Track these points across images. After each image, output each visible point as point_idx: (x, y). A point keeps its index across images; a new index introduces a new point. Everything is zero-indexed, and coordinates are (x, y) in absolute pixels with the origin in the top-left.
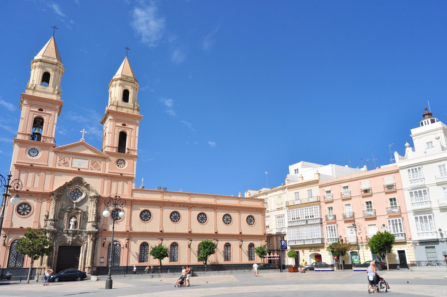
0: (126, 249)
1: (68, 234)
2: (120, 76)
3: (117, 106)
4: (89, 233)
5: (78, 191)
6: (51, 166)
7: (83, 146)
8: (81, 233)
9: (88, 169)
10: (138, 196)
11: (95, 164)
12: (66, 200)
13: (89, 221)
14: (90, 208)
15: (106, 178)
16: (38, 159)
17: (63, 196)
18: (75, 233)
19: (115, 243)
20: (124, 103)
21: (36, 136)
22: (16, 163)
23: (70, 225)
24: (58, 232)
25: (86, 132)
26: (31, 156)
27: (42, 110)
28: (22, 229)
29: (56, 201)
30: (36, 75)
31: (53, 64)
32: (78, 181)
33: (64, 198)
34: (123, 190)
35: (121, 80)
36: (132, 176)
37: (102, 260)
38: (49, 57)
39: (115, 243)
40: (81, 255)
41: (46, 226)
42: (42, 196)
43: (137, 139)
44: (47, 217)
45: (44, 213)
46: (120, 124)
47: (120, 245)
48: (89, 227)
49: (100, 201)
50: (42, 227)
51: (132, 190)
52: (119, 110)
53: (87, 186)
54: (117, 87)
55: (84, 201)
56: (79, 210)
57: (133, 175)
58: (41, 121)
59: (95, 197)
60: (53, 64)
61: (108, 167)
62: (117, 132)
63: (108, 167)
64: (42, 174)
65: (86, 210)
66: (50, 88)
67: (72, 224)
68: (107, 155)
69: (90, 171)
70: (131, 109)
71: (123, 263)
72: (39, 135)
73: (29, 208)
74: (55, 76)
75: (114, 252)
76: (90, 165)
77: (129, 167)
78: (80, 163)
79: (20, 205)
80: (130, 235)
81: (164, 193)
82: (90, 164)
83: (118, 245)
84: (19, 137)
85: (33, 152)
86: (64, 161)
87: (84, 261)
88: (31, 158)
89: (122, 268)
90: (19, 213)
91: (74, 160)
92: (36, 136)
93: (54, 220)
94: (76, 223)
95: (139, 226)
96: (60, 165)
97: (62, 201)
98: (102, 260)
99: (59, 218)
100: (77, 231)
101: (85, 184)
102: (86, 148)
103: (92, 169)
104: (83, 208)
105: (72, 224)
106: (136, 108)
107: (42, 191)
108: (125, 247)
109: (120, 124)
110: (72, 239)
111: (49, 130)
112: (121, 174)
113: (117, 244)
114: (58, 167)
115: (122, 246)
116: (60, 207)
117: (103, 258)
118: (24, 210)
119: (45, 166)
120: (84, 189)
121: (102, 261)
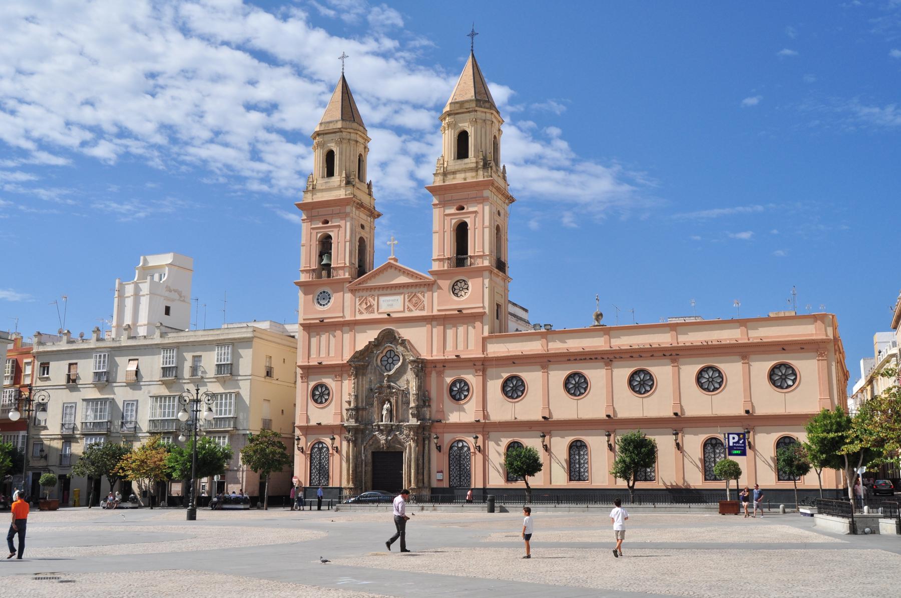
0: (479, 456)
1: (381, 431)
4: (410, 428)
6: (348, 317)
7: (393, 270)
8: (399, 428)
9: (404, 311)
10: (497, 349)
11: (414, 300)
14: (410, 382)
15: (434, 323)
18: (389, 430)
19: (460, 445)
22: (302, 322)
32: (388, 337)
34: (467, 342)
36: (481, 310)
37: (440, 476)
40: (405, 467)
42: (337, 371)
46: (453, 210)
49: (423, 367)
51: (484, 339)
53: (403, 343)
55: (401, 372)
57: (483, 307)
59: (414, 361)
61: (439, 301)
63: (439, 301)
64: (338, 333)
69: (407, 314)
71: (477, 482)
72: (328, 267)
75: (459, 462)
76: (407, 303)
78: (390, 303)
79: (315, 388)
80: (485, 428)
81: (549, 336)
82: (407, 300)
83: (466, 449)
85: (324, 297)
90: (316, 401)
91: (382, 299)
94: (390, 411)
95: (502, 410)
96: (361, 313)
97: (369, 375)
98: (440, 476)
99: (367, 404)
102: (397, 271)
103: (410, 310)
104: (402, 384)
110: (386, 440)
112: (460, 311)
113: (463, 446)
115: (472, 450)
117: (442, 472)
119: (341, 319)
120: (400, 349)
121: (439, 478)
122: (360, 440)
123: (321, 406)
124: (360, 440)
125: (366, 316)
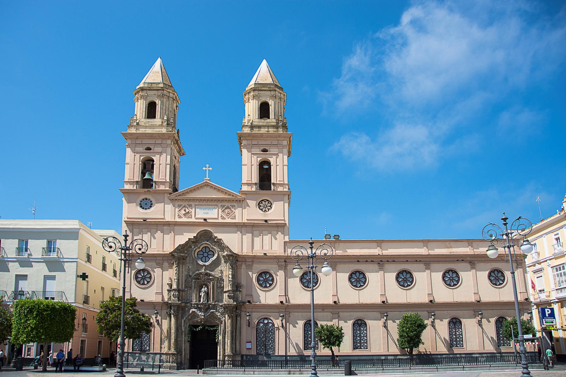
0: (282, 331)
2: (253, 86)
7: (208, 188)
8: (214, 307)
9: (217, 219)
12: (193, 263)
13: (225, 290)
14: (225, 272)
15: (244, 229)
16: (152, 211)
17: (188, 258)
18: (206, 308)
19: (266, 322)
20: (263, 121)
21: (147, 184)
22: (127, 220)
24: (186, 306)
25: (211, 169)
26: (143, 208)
27: (150, 149)
28: (142, 303)
29: (178, 266)
30: (140, 108)
31: (158, 90)
32: (206, 236)
33: (190, 260)
34: (272, 245)
35: (254, 90)
36: (283, 222)
37: (249, 346)
38: (152, 83)
39: (266, 322)
41: (170, 299)
42: (162, 260)
43: (286, 168)
44: (171, 286)
45: (166, 281)
46: (258, 151)
47: (273, 325)
48: (226, 300)
50: (166, 300)
52: (256, 131)
53: (219, 243)
54: (250, 101)
55: (217, 263)
56: (210, 275)
57: (284, 220)
58: (151, 163)
60: (158, 90)
62: (256, 161)
65: (220, 275)
66: (157, 121)
67: (202, 294)
68: (243, 196)
69: (220, 220)
70: (273, 126)
71: (280, 351)
73: (149, 276)
74: (162, 103)
75: (265, 336)
76: (220, 213)
77: (278, 211)
80: (286, 310)
81: (337, 245)
83: (270, 325)
84: (127, 187)
85: (146, 204)
86: (185, 211)
87: (225, 348)
88: (144, 211)
89: (278, 359)
92: (147, 184)
93: (178, 290)
94: (207, 294)
95: (299, 296)
96: (180, 217)
98: (249, 346)
99: (186, 287)
100: (210, 304)
102: (212, 190)
103: (223, 218)
104: (216, 273)
105: (202, 294)
106: (280, 124)
107: (162, 253)
108: (281, 328)
109: (258, 151)
111: (161, 173)
114: (177, 220)
115: (276, 326)
116: (185, 273)
117: (250, 342)
118: (144, 278)
121: (249, 346)
122: (180, 315)
123: (143, 286)
124: (180, 315)
125: (184, 219)
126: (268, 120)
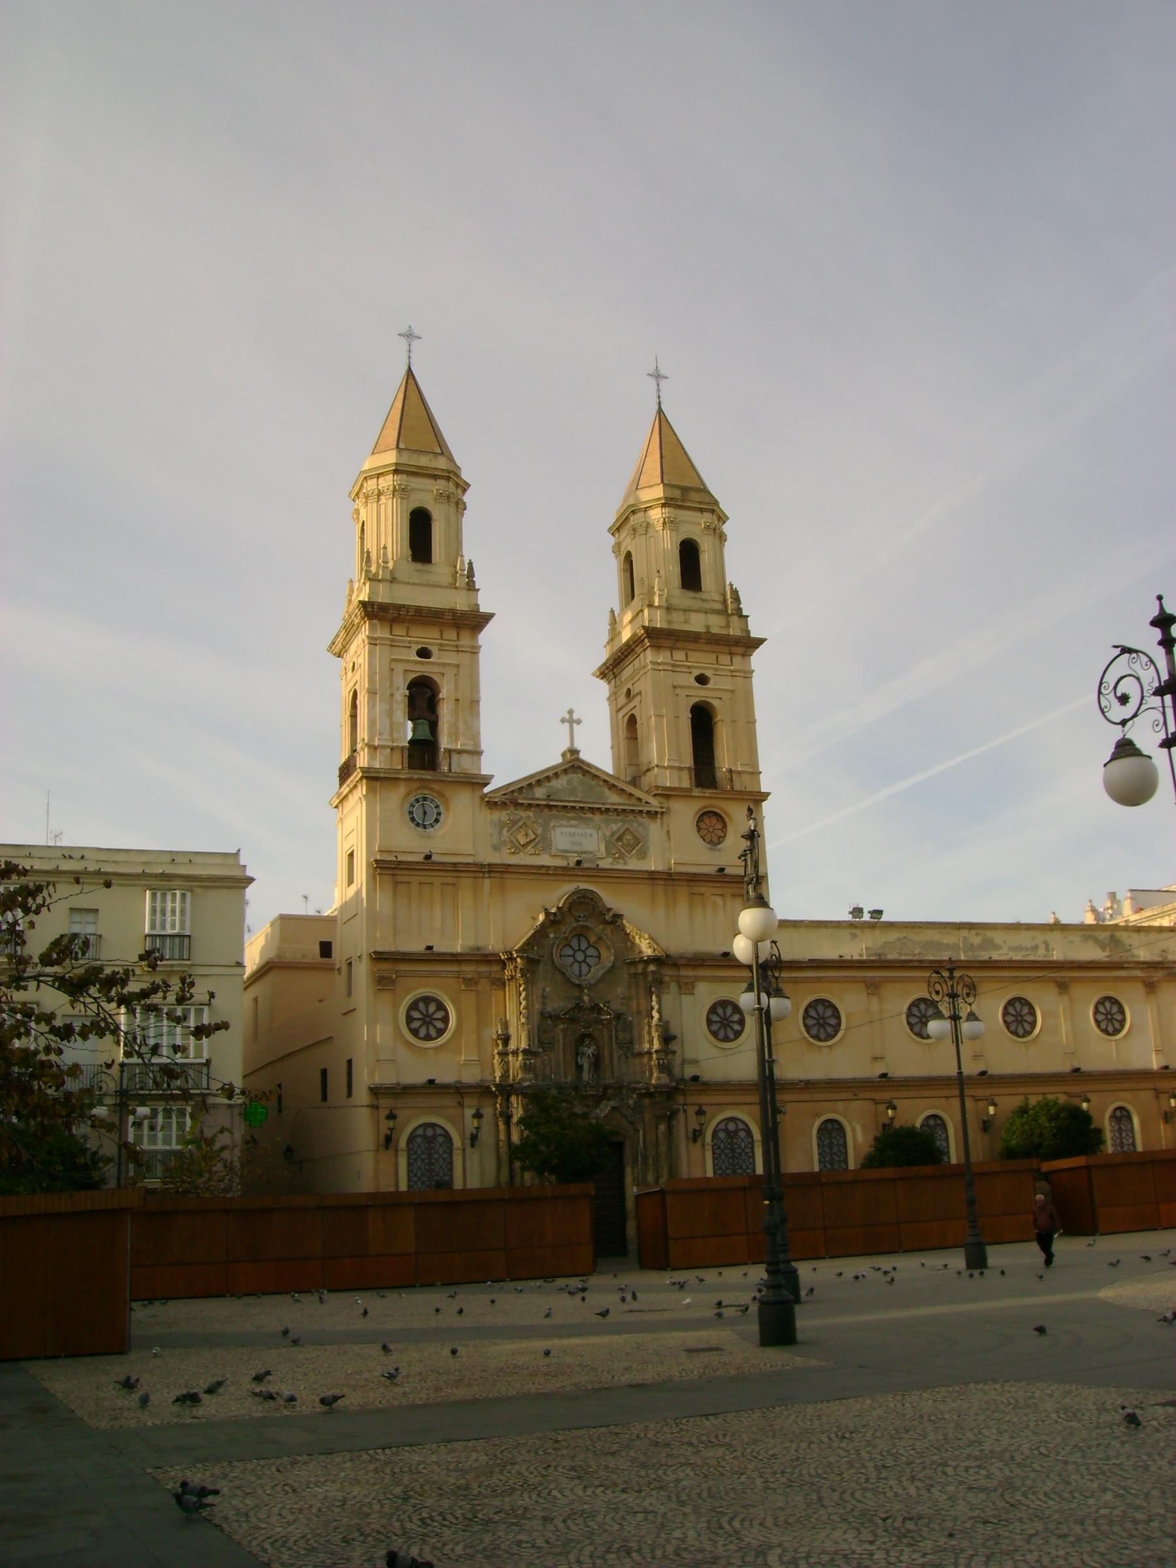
3: (669, 609)
5: (584, 945)
17: (541, 966)
23: (579, 1068)
41: (505, 1075)
101: (608, 917)
126: (699, 595)
